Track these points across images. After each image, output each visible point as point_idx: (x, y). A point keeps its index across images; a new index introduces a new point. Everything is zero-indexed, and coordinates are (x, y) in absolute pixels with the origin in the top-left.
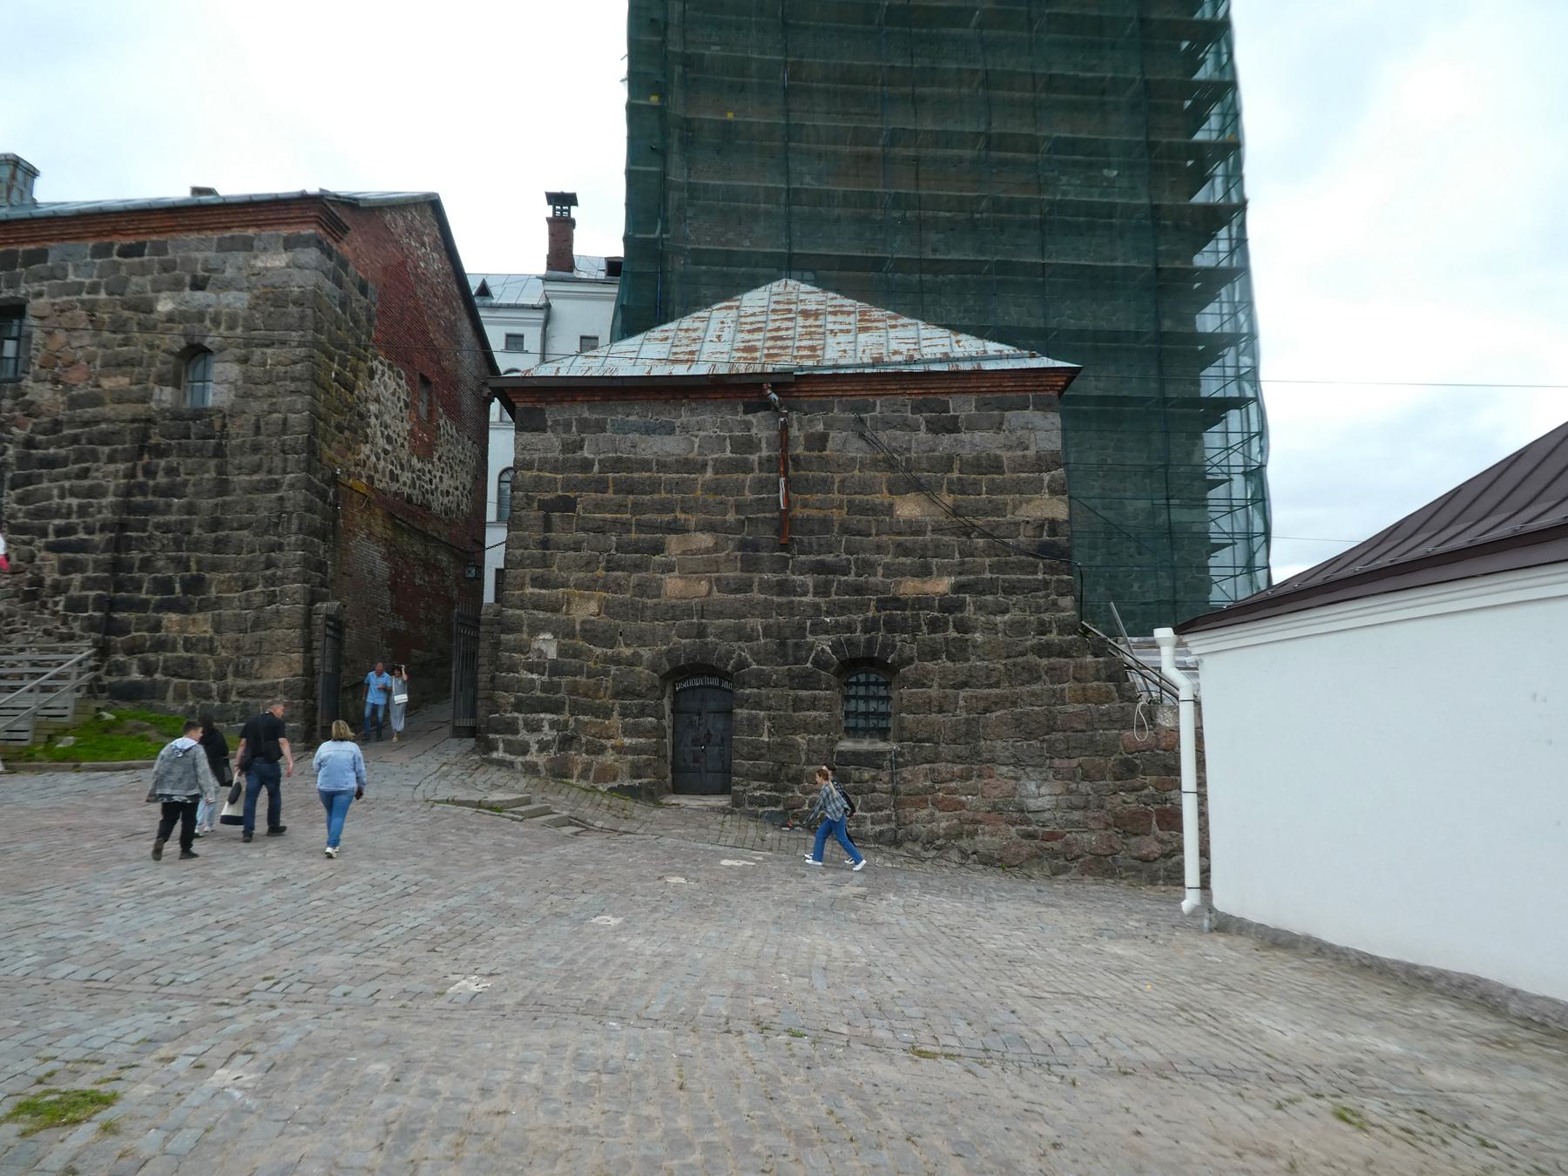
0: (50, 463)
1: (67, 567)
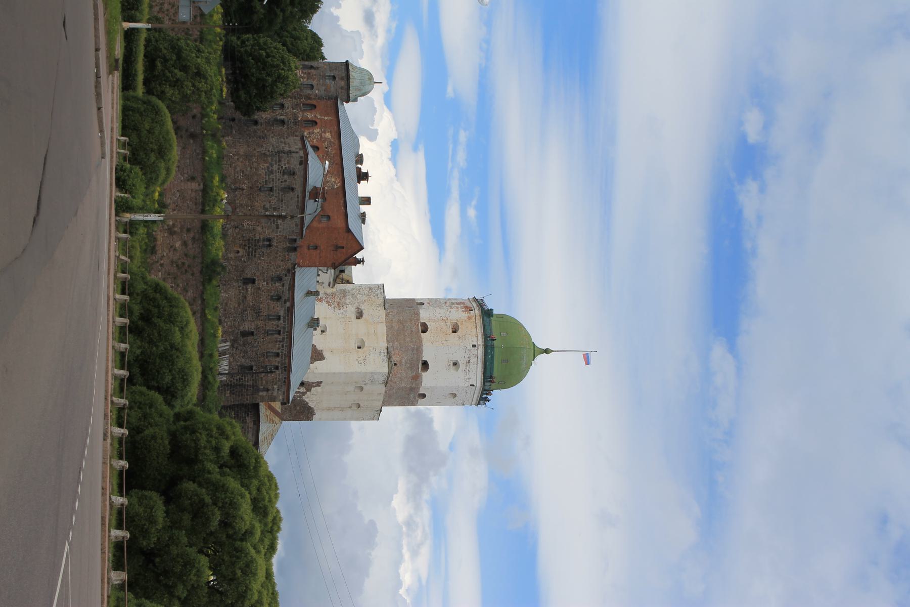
0: (252, 376)
1: (237, 380)
